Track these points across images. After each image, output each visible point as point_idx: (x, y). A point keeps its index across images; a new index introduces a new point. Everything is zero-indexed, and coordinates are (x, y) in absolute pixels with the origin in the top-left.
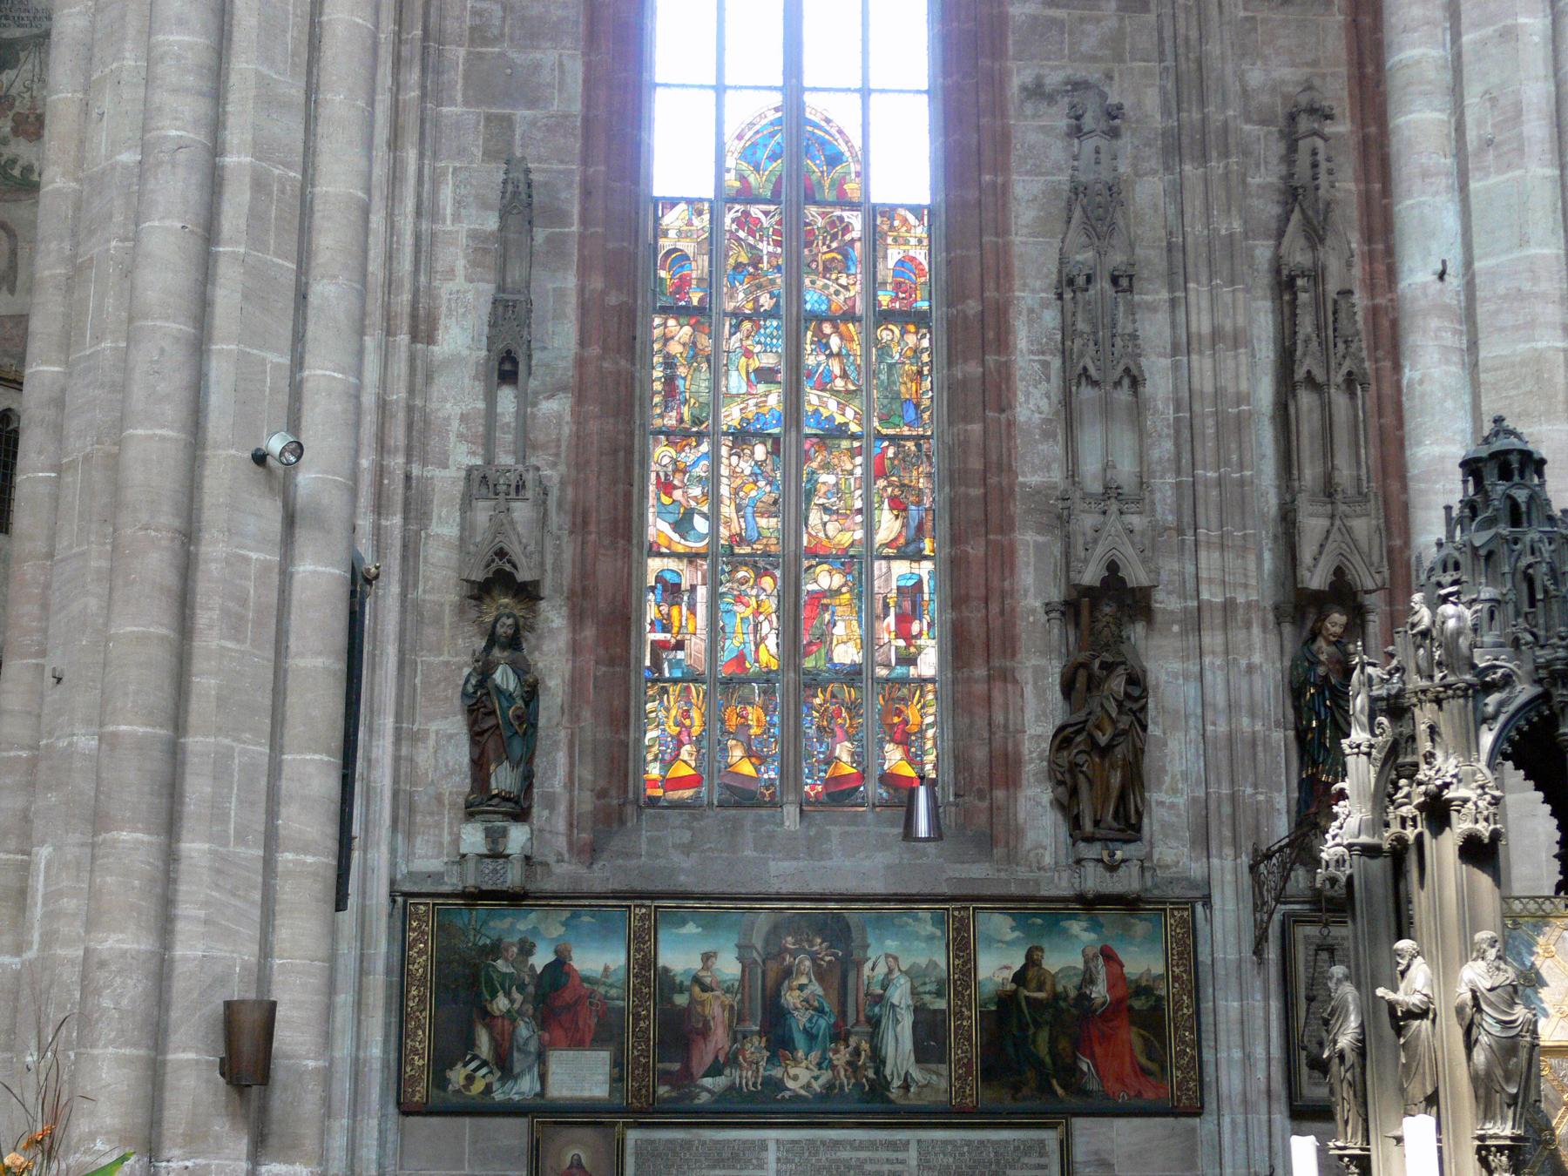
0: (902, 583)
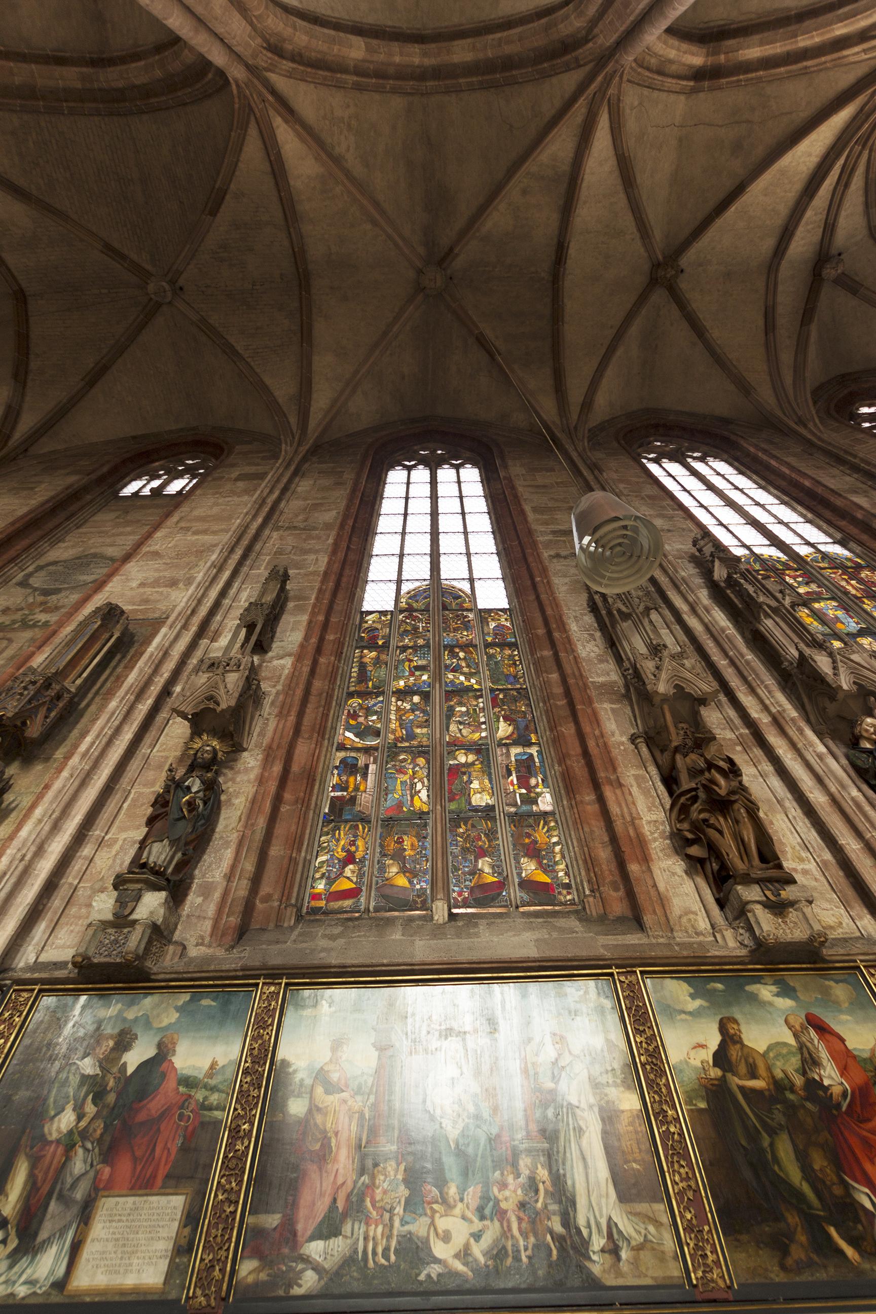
0: (519, 758)
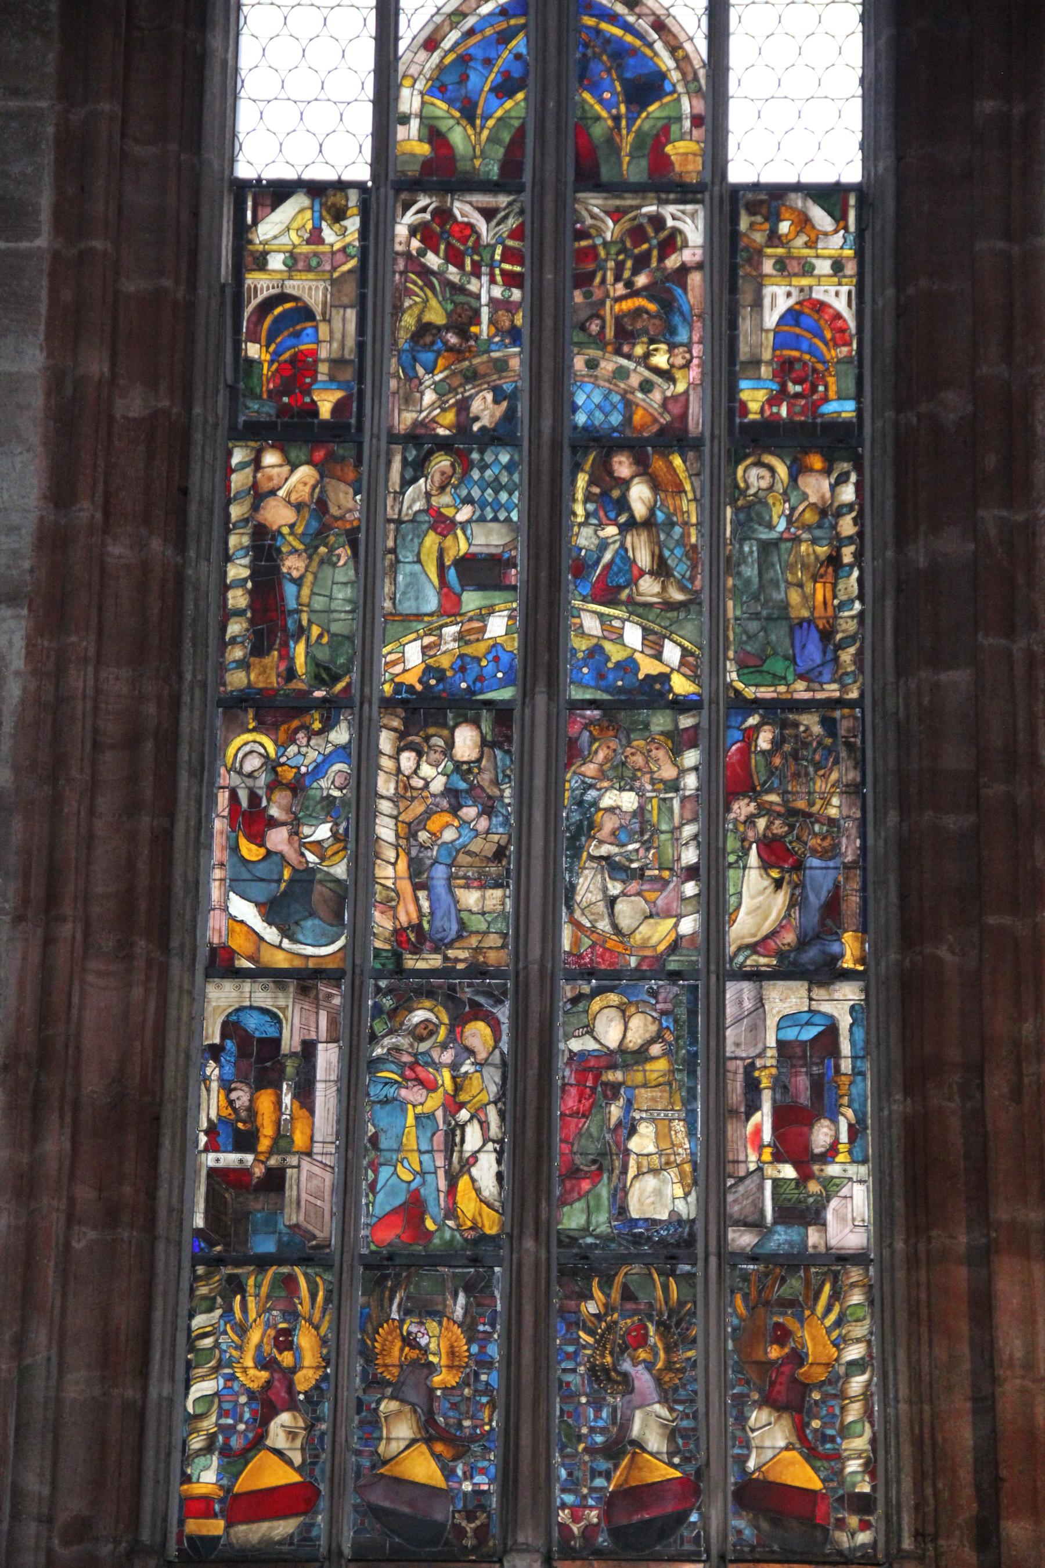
0: (790, 1034)
